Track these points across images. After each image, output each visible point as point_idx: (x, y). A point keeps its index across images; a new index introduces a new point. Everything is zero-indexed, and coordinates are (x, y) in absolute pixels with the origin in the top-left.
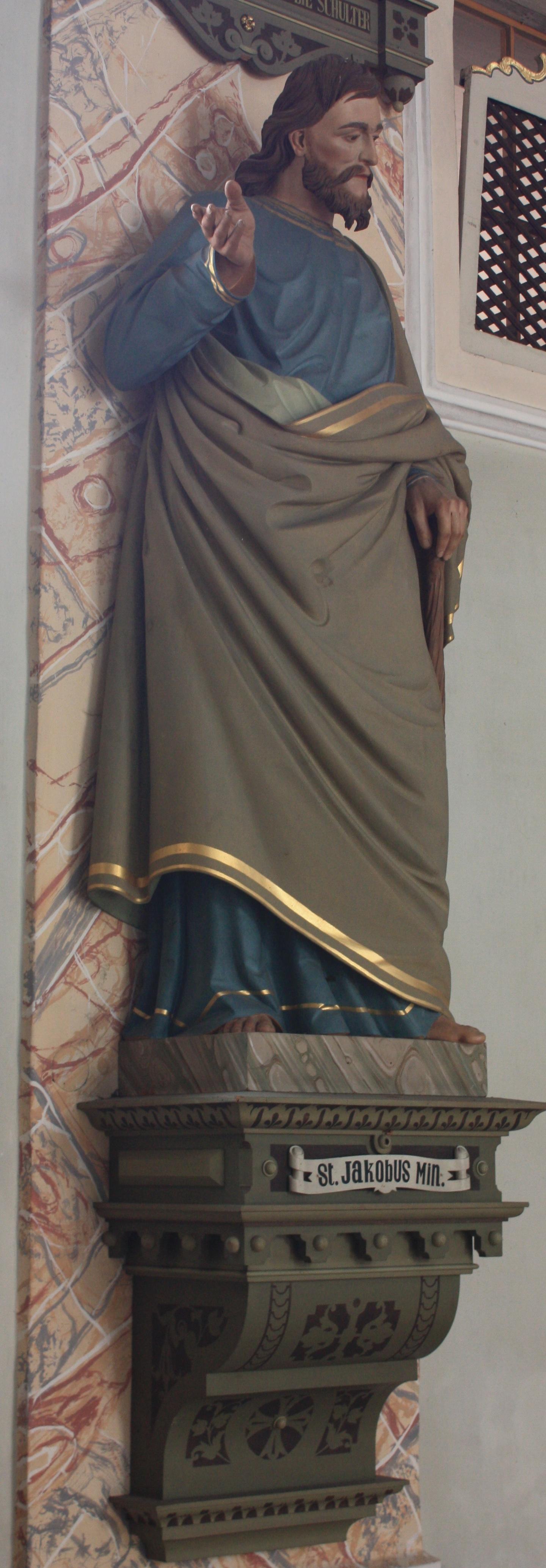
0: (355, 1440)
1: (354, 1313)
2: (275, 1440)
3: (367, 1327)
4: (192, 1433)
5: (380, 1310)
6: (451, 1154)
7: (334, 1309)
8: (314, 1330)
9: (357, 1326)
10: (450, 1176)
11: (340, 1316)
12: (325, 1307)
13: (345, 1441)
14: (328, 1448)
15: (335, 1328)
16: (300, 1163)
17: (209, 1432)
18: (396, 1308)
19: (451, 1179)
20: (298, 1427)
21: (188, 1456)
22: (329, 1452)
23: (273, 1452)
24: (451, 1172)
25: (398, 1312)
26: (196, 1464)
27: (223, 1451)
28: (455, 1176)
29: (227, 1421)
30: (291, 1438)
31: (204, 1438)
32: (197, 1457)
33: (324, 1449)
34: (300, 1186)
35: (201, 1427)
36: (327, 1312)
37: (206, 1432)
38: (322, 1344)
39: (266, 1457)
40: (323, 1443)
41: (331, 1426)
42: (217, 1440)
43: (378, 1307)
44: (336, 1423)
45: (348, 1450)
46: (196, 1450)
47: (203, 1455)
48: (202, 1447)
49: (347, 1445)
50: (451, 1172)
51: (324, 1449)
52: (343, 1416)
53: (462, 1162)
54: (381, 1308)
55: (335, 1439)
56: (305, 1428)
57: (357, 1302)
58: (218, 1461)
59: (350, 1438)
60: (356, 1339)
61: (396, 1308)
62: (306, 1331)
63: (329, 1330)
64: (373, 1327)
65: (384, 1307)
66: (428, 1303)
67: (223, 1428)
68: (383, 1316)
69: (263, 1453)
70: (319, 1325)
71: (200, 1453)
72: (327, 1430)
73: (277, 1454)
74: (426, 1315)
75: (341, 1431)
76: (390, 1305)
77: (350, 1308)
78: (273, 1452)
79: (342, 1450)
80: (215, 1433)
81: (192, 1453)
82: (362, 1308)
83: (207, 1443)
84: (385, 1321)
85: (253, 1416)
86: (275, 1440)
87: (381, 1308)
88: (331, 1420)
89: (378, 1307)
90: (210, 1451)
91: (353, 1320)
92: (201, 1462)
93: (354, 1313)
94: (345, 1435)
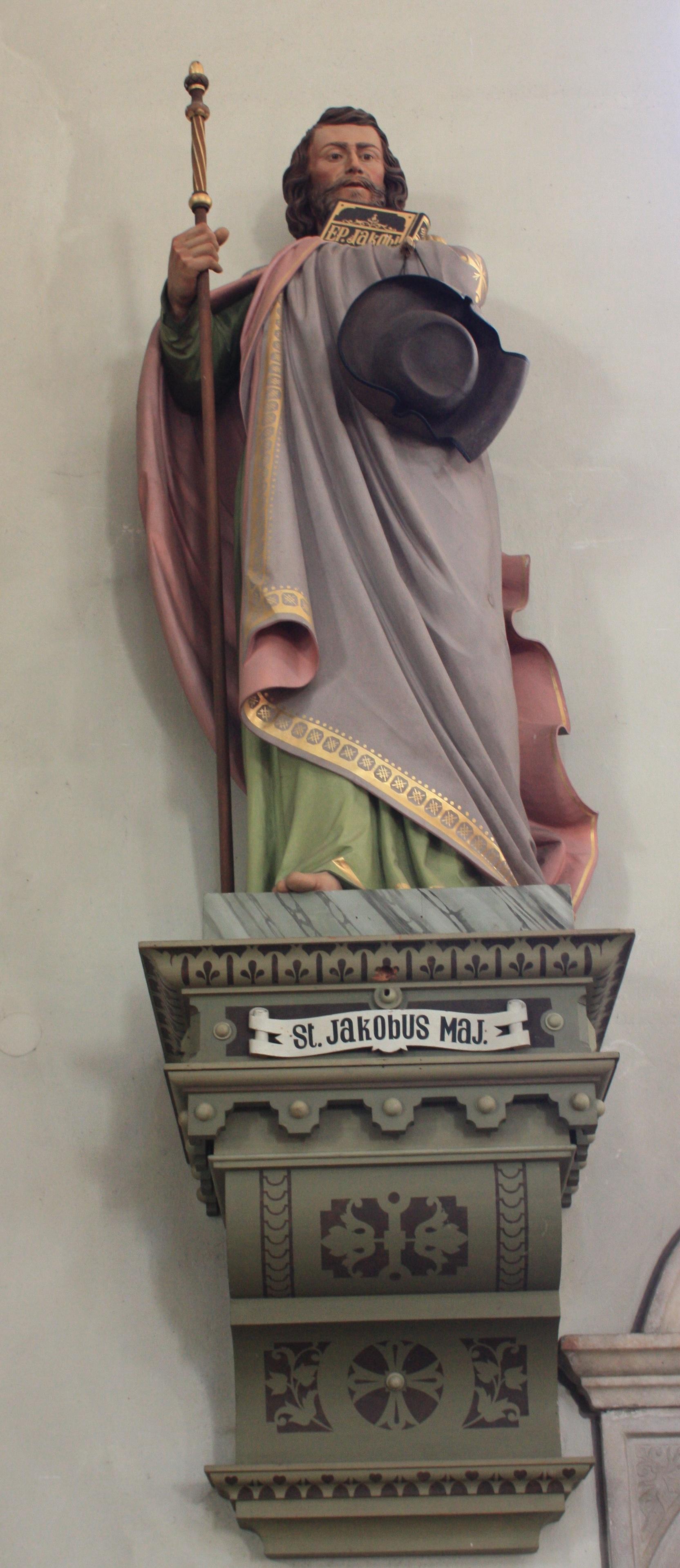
0: (525, 1412)
1: (394, 1212)
2: (396, 1404)
3: (420, 1229)
4: (269, 1391)
6: (501, 1006)
7: (359, 1204)
8: (335, 1230)
9: (403, 1229)
10: (500, 1031)
11: (370, 1212)
12: (347, 1201)
13: (507, 1412)
15: (370, 1230)
17: (295, 1392)
18: (459, 1203)
20: (429, 1389)
21: (270, 1418)
22: (483, 1424)
23: (397, 1420)
26: (281, 1430)
27: (320, 1415)
28: (505, 1030)
29: (315, 1375)
30: (421, 1405)
31: (288, 1396)
32: (283, 1422)
33: (474, 1420)
36: (349, 1207)
37: (289, 1391)
38: (360, 1250)
39: (386, 1426)
41: (482, 1391)
42: (309, 1401)
43: (429, 1203)
44: (489, 1389)
45: (515, 1424)
46: (282, 1410)
47: (291, 1420)
48: (288, 1409)
49: (511, 1417)
51: (474, 1420)
52: (496, 1377)
53: (517, 1012)
54: (435, 1204)
55: (491, 1410)
56: (440, 1391)
58: (312, 1427)
59: (513, 1406)
60: (410, 1246)
61: (459, 1203)
62: (325, 1233)
63: (360, 1231)
64: (430, 1230)
65: (439, 1205)
66: (511, 1199)
67: (314, 1386)
68: (441, 1215)
69: (382, 1420)
70: (343, 1225)
71: (287, 1416)
72: (476, 1396)
73: (402, 1423)
74: (512, 1214)
76: (448, 1202)
77: (385, 1205)
78: (397, 1420)
80: (303, 1391)
82: (404, 1204)
85: (351, 1371)
86: (396, 1404)
87: (435, 1204)
88: (478, 1383)
89: (429, 1203)
90: (303, 1415)
92: (291, 1427)
93: (394, 1212)
94: (505, 1404)
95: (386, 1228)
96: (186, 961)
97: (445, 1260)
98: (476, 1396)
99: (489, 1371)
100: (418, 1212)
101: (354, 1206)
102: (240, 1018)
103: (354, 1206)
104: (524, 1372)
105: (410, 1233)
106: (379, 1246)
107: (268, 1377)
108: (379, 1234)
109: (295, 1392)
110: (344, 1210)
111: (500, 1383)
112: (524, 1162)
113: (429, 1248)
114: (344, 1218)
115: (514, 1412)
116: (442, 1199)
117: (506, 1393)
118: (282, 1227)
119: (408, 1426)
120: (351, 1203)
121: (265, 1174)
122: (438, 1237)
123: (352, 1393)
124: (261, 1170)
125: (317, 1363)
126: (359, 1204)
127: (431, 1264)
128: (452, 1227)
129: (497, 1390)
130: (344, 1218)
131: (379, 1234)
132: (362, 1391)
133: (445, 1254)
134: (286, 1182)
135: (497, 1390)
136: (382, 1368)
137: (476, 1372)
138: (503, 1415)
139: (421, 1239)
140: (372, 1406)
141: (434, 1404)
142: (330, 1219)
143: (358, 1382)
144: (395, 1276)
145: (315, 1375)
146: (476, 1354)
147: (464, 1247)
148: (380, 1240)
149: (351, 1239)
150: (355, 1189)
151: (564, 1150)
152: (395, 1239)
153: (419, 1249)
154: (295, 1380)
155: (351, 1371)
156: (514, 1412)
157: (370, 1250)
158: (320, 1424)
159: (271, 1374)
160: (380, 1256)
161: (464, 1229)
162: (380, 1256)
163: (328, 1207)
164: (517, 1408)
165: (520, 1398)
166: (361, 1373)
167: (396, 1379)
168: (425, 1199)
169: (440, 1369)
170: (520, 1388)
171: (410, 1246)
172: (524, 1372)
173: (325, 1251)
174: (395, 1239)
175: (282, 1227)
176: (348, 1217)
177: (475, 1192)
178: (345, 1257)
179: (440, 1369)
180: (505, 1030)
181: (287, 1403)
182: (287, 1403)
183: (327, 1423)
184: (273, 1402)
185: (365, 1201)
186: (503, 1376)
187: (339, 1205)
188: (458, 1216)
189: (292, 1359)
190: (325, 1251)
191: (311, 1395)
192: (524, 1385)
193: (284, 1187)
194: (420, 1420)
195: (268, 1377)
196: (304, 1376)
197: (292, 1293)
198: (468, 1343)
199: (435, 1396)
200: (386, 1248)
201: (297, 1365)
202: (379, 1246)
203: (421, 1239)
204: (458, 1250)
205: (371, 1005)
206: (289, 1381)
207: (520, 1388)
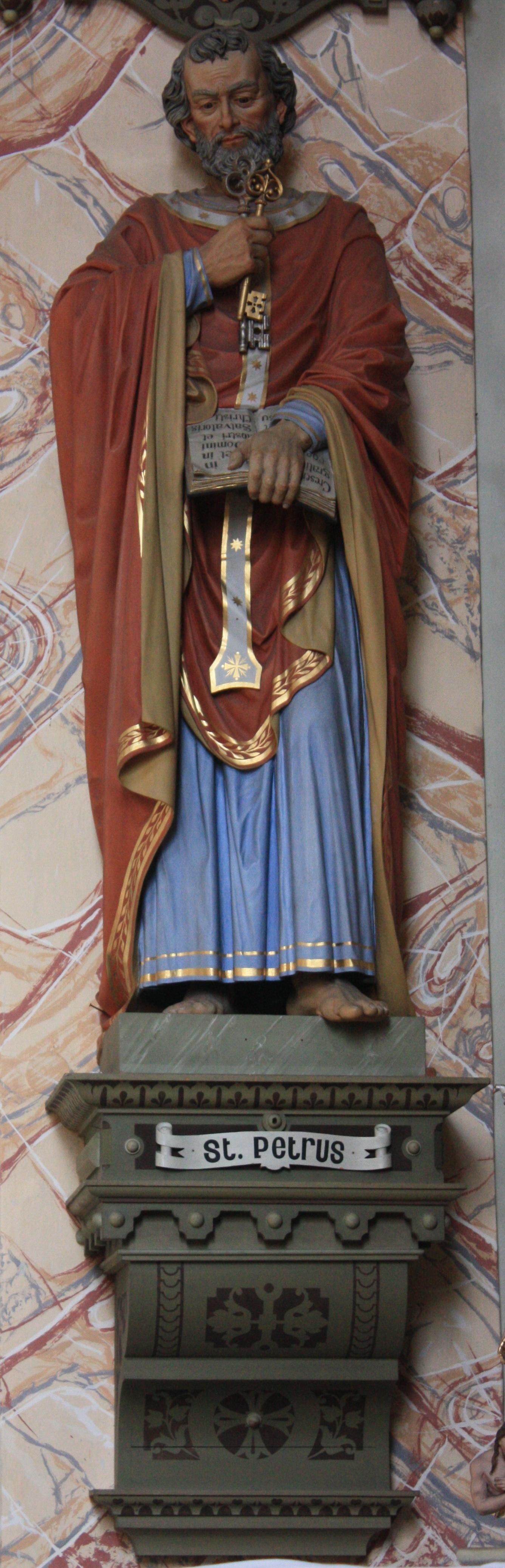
0: (360, 1447)
1: (269, 1300)
3: (290, 1313)
4: (147, 1424)
5: (301, 1298)
6: (369, 1132)
7: (239, 1293)
8: (219, 1314)
10: (368, 1154)
12: (230, 1290)
13: (344, 1447)
14: (325, 1453)
16: (164, 1136)
17: (169, 1425)
18: (323, 1295)
19: (368, 1157)
20: (281, 1426)
22: (325, 1456)
24: (368, 1151)
25: (326, 1301)
26: (155, 1457)
27: (189, 1445)
28: (372, 1153)
29: (187, 1413)
30: (274, 1440)
31: (163, 1429)
33: (317, 1452)
34: (163, 1160)
35: (156, 1420)
39: (243, 1456)
40: (317, 1446)
42: (180, 1433)
43: (298, 1293)
44: (332, 1427)
45: (351, 1457)
48: (162, 1439)
49: (349, 1451)
50: (368, 1151)
55: (332, 1444)
56: (290, 1428)
57: (269, 1288)
60: (280, 1328)
61: (323, 1295)
63: (238, 1314)
64: (297, 1315)
65: (306, 1295)
67: (185, 1422)
68: (307, 1304)
70: (226, 1309)
71: (162, 1446)
72: (320, 1434)
73: (257, 1454)
75: (338, 1436)
76: (314, 1293)
77: (261, 1294)
79: (342, 1456)
80: (176, 1426)
81: (152, 1444)
82: (277, 1294)
83: (167, 1434)
84: (311, 1309)
88: (323, 1422)
89: (298, 1293)
93: (269, 1300)
94: (344, 1440)
95: (261, 1312)
96: (105, 1090)
97: (308, 1338)
98: (320, 1434)
99: (332, 1414)
100: (289, 1299)
101: (235, 1293)
102: (147, 1134)
103: (235, 1293)
104: (362, 1415)
106: (254, 1327)
107: (147, 1414)
108: (255, 1316)
109: (169, 1425)
110: (227, 1298)
111: (341, 1422)
112: (378, 1262)
113: (295, 1329)
114: (227, 1303)
115: (351, 1447)
116: (308, 1290)
117: (345, 1431)
118: (175, 1309)
119: (262, 1456)
120: (233, 1291)
121: (162, 1265)
122: (303, 1321)
123: (217, 1428)
124: (159, 1263)
125: (190, 1405)
126: (239, 1293)
127: (296, 1341)
128: (317, 1313)
129: (338, 1429)
130: (227, 1303)
131: (255, 1316)
132: (225, 1427)
133: (308, 1334)
134: (179, 1272)
135: (338, 1429)
136: (244, 1409)
137: (322, 1414)
138: (341, 1450)
139: (289, 1321)
140: (232, 1440)
141: (285, 1438)
142: (215, 1304)
143: (222, 1419)
144: (265, 1347)
145: (187, 1413)
147: (324, 1329)
148: (254, 1322)
149: (232, 1320)
150: (237, 1279)
151: (414, 1255)
152: (267, 1322)
153: (287, 1330)
154: (170, 1417)
155: (217, 1411)
156: (351, 1447)
157: (246, 1329)
159: (150, 1411)
160: (255, 1333)
161: (326, 1315)
162: (255, 1333)
163: (214, 1294)
164: (352, 1443)
165: (357, 1436)
166: (226, 1412)
168: (294, 1290)
169: (292, 1412)
170: (357, 1427)
171: (280, 1328)
172: (362, 1415)
173: (209, 1328)
174: (267, 1322)
175: (175, 1309)
176: (230, 1303)
177: (336, 1284)
178: (224, 1333)
179: (292, 1412)
180: (372, 1153)
181: (161, 1434)
182: (161, 1434)
184: (150, 1434)
185: (245, 1290)
186: (344, 1418)
187: (223, 1293)
188: (321, 1305)
190: (209, 1328)
191: (182, 1429)
192: (361, 1425)
193: (178, 1276)
194: (273, 1452)
195: (147, 1414)
196: (177, 1413)
197: (177, 1354)
199: (286, 1432)
200: (260, 1328)
201: (173, 1406)
202: (254, 1327)
203: (289, 1321)
204: (318, 1331)
205: (259, 1127)
206: (164, 1417)
207: (357, 1427)
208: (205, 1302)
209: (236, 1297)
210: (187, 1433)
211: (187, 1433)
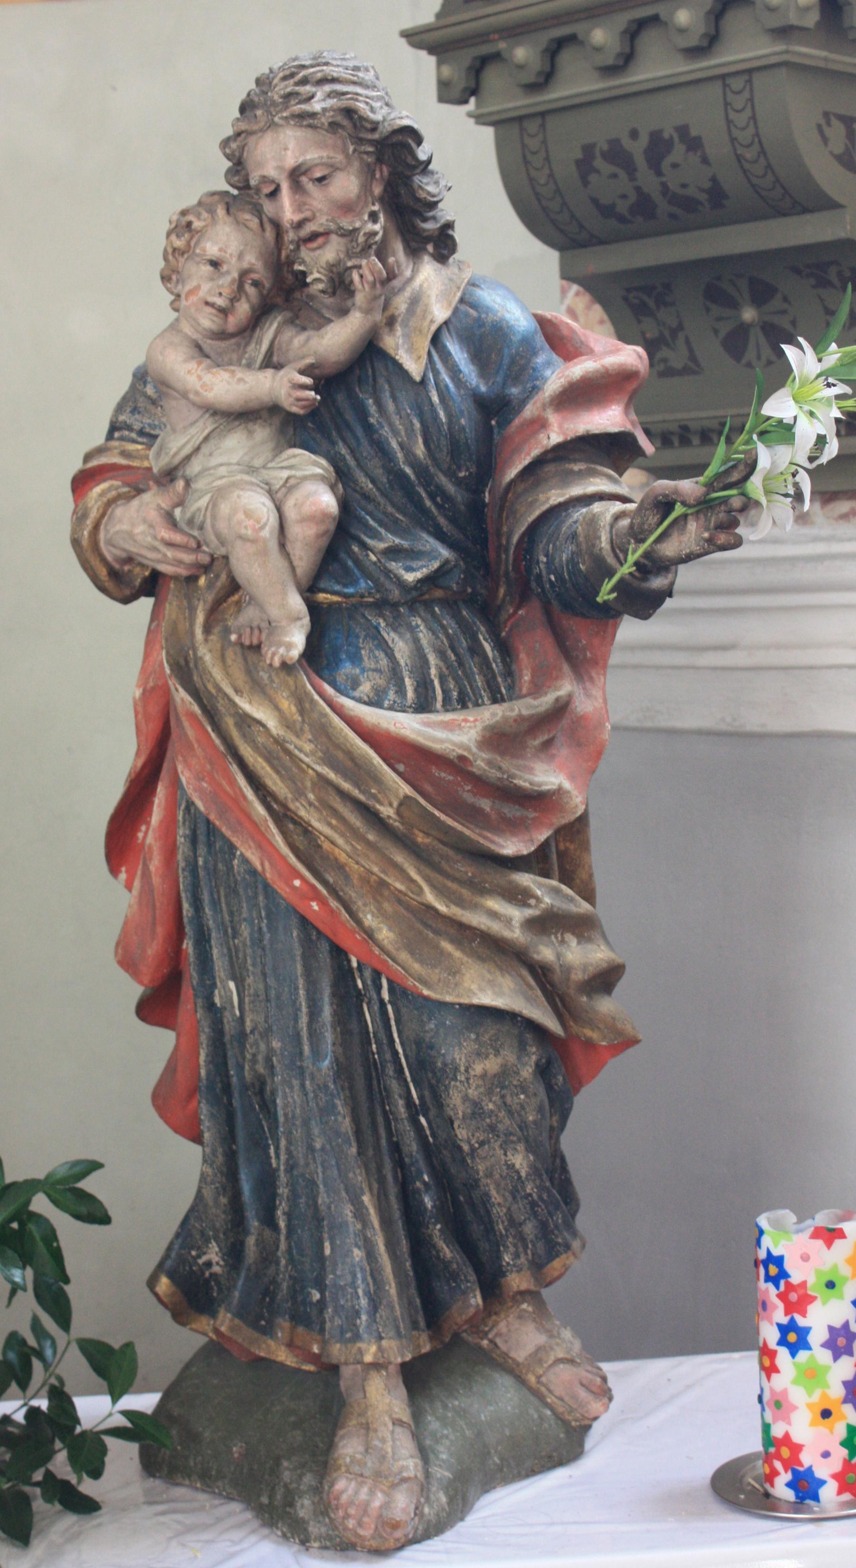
7: (605, 147)
11: (616, 154)
15: (622, 174)
18: (694, 133)
23: (759, 357)
27: (693, 358)
32: (662, 367)
39: (749, 365)
43: (666, 135)
54: (671, 138)
57: (634, 134)
58: (685, 371)
61: (694, 133)
62: (586, 183)
63: (614, 176)
64: (675, 166)
67: (680, 327)
70: (598, 172)
71: (664, 360)
76: (683, 131)
77: (627, 143)
78: (759, 357)
80: (674, 333)
82: (644, 140)
83: (667, 345)
89: (666, 135)
91: (640, 161)
95: (635, 170)
100: (658, 147)
105: (659, 173)
112: (750, 71)
122: (686, 173)
123: (716, 332)
126: (605, 147)
132: (725, 328)
136: (734, 305)
142: (585, 166)
146: (813, 281)
150: (602, 128)
158: (692, 368)
163: (579, 155)
167: (749, 314)
168: (660, 132)
169: (785, 299)
181: (664, 348)
183: (698, 365)
189: (651, 304)
191: (681, 336)
195: (639, 322)
198: (797, 271)
208: (573, 168)
209: (604, 155)
210: (688, 342)
211: (688, 342)
